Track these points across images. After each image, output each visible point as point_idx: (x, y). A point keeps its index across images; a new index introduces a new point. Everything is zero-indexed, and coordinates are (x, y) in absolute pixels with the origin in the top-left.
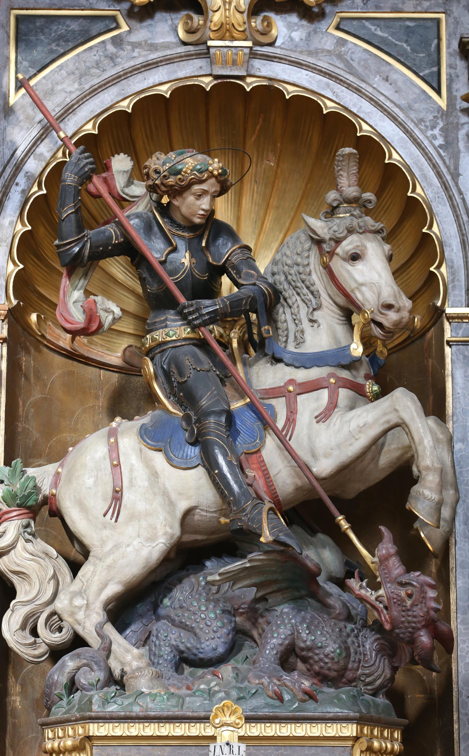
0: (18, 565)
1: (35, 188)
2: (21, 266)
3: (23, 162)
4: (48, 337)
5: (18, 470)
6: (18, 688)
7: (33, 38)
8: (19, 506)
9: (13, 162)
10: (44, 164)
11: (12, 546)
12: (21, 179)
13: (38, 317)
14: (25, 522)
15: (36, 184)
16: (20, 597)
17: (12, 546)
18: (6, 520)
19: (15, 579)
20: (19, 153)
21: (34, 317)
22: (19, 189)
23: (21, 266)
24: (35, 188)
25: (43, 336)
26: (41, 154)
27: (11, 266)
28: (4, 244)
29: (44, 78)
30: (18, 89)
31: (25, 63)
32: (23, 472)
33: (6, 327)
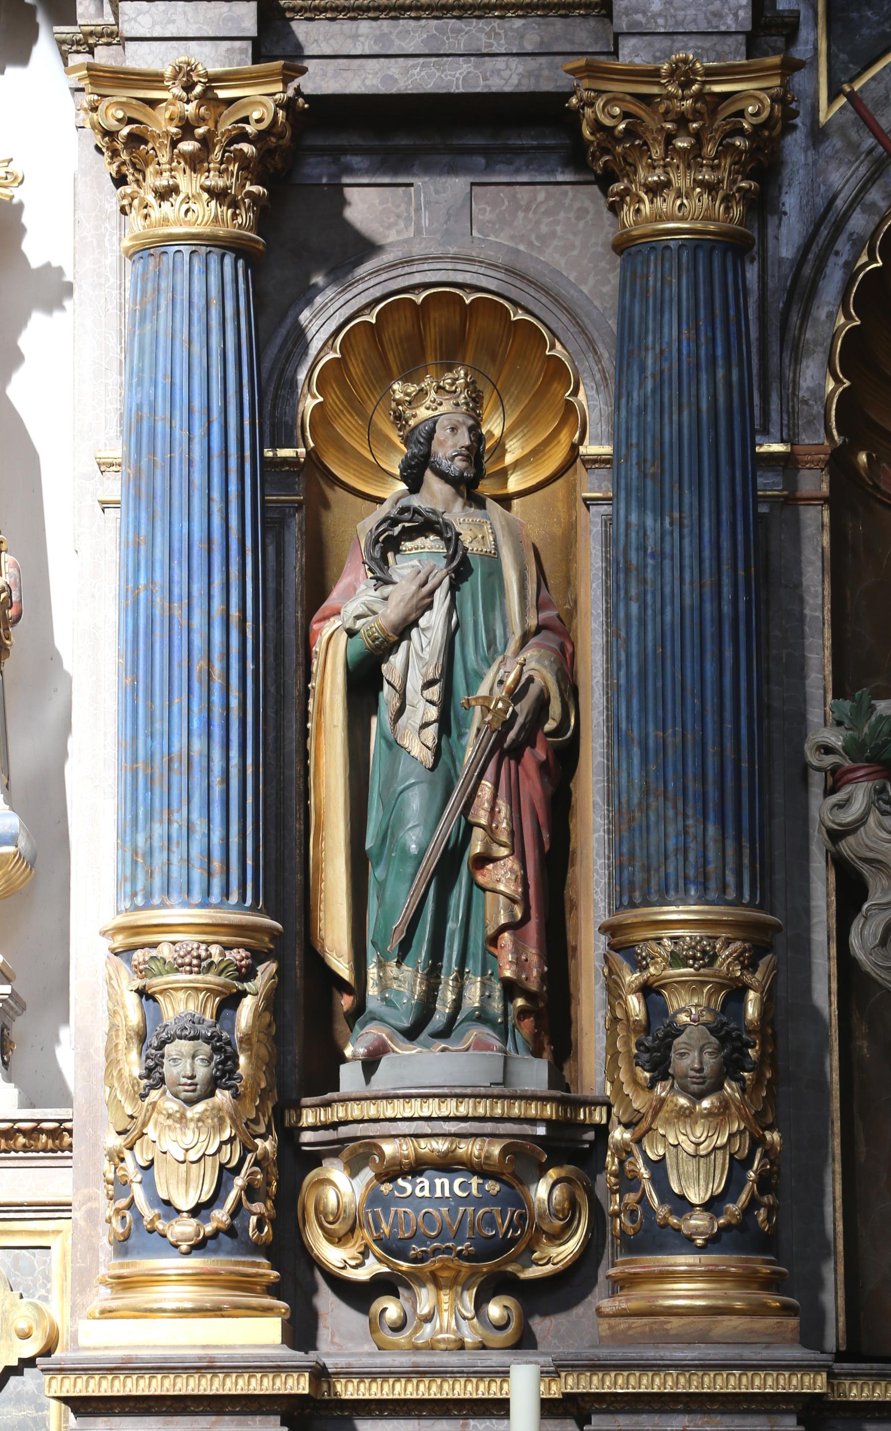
0: (871, 850)
1: (864, 259)
2: (847, 383)
3: (846, 216)
4: (883, 487)
5: (865, 705)
6: (864, 1029)
7: (855, 15)
8: (868, 760)
9: (831, 217)
10: (877, 219)
11: (861, 821)
12: (843, 246)
13: (869, 457)
14: (878, 784)
15: (865, 251)
16: (875, 897)
17: (861, 821)
18: (849, 782)
19: (866, 870)
20: (839, 202)
21: (863, 458)
22: (841, 261)
23: (847, 383)
24: (864, 259)
25: (876, 487)
26: (873, 204)
27: (831, 385)
28: (820, 349)
29: (873, 78)
30: (831, 99)
31: (843, 56)
32: (872, 708)
33: (826, 479)
